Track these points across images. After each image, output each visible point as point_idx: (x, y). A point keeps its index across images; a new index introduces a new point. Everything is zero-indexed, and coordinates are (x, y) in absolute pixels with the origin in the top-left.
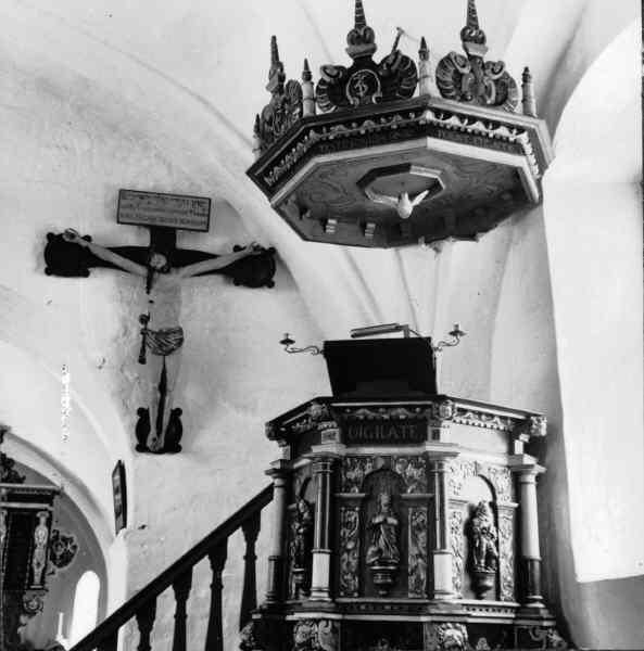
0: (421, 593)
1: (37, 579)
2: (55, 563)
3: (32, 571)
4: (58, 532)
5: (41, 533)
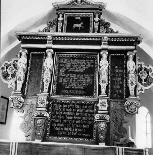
3: (128, 88)
4: (141, 65)
5: (131, 65)
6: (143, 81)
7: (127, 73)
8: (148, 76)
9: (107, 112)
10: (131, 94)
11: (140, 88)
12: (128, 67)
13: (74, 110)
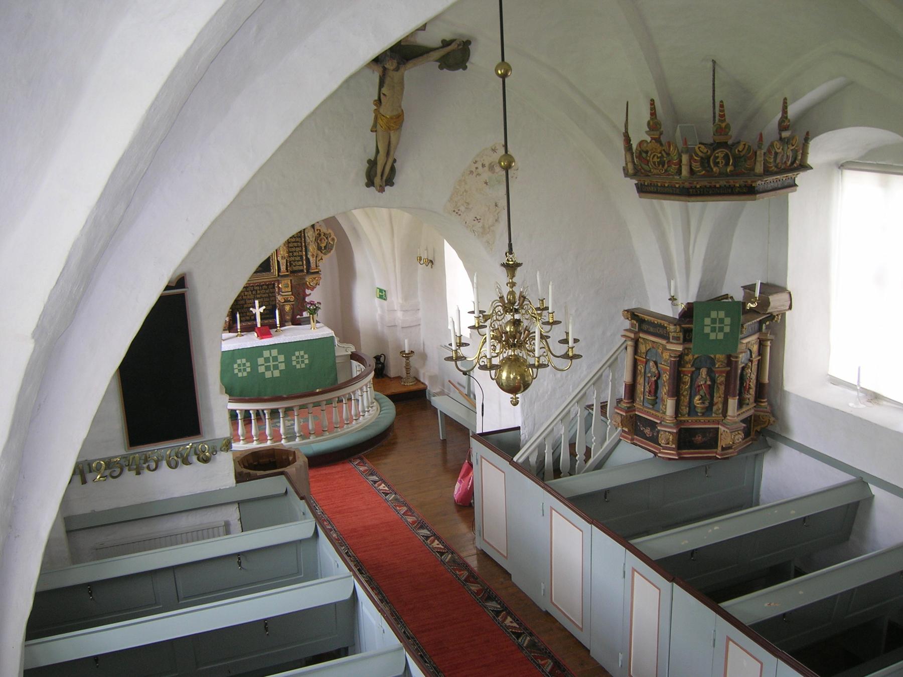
0: (719, 414)
1: (313, 265)
2: (322, 252)
3: (308, 260)
4: (320, 230)
6: (323, 248)
7: (307, 244)
8: (327, 243)
9: (291, 293)
10: (312, 266)
11: (320, 258)
12: (307, 238)
13: (254, 292)
